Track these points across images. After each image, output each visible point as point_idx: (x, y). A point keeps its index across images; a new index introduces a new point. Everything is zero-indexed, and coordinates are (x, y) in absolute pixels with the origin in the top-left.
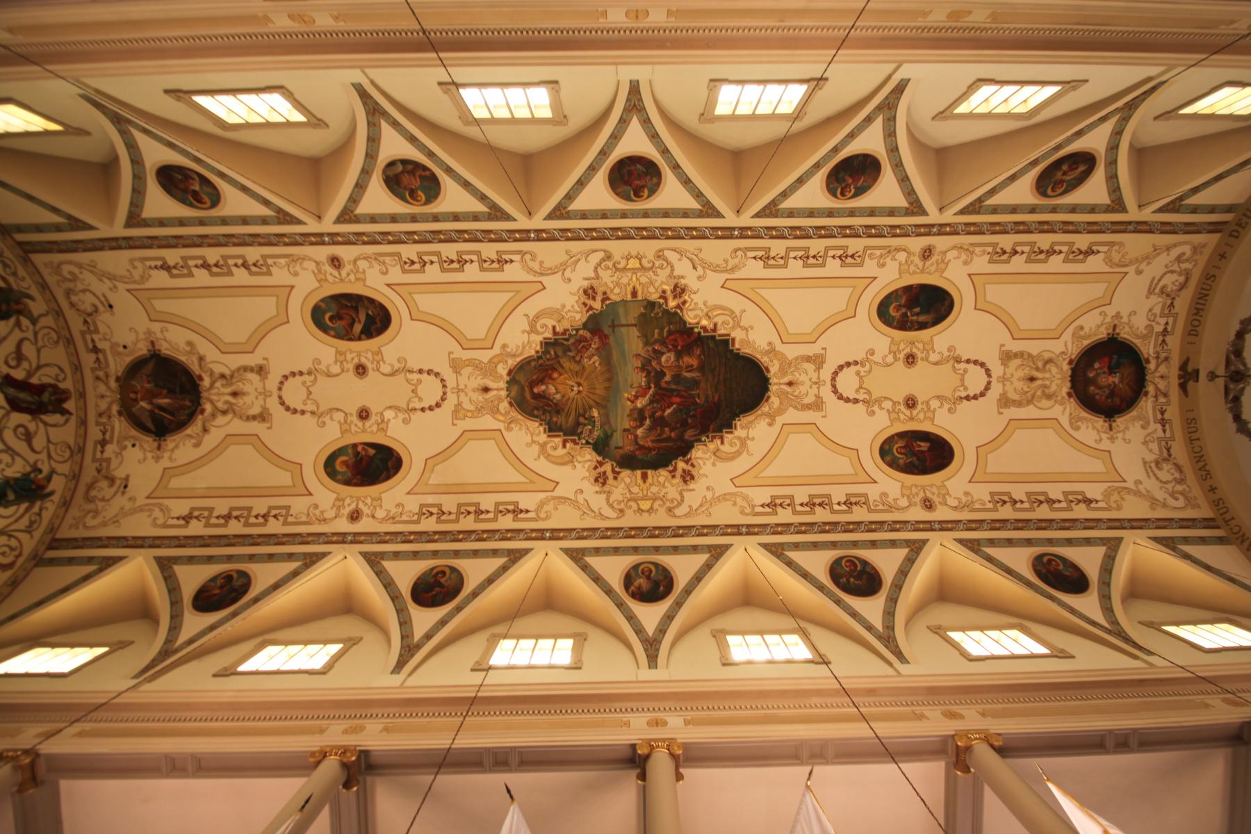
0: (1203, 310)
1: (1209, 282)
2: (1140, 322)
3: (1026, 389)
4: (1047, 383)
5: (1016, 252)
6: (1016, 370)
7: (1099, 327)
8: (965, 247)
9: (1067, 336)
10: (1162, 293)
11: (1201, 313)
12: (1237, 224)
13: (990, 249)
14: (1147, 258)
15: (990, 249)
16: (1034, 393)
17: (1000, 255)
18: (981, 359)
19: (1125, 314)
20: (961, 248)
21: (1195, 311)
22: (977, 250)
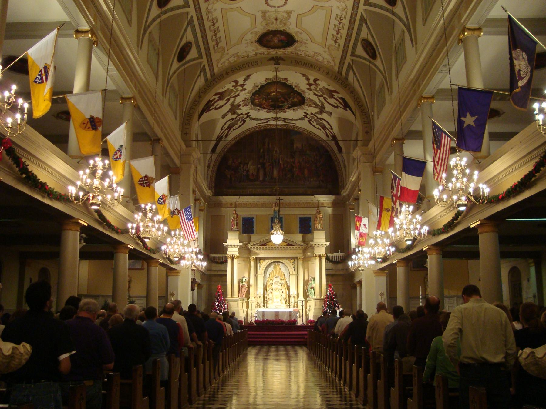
0: (306, 66)
1: (318, 68)
2: (302, 48)
3: (271, 18)
4: (274, 24)
5: (340, 23)
6: (281, 15)
7: (302, 38)
8: (346, 10)
9: (297, 30)
10: (315, 55)
11: (305, 66)
12: (339, 79)
13: (343, 16)
14: (331, 55)
15: (343, 16)
16: (268, 20)
17: (340, 19)
18: (287, 5)
19: (306, 45)
20: (346, 9)
21: (305, 63)
22: (344, 13)
